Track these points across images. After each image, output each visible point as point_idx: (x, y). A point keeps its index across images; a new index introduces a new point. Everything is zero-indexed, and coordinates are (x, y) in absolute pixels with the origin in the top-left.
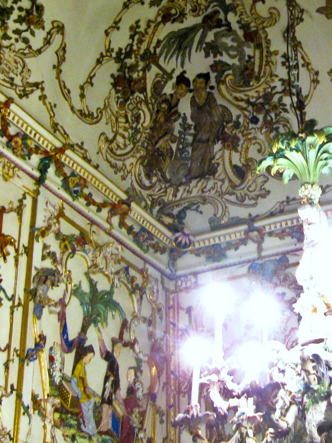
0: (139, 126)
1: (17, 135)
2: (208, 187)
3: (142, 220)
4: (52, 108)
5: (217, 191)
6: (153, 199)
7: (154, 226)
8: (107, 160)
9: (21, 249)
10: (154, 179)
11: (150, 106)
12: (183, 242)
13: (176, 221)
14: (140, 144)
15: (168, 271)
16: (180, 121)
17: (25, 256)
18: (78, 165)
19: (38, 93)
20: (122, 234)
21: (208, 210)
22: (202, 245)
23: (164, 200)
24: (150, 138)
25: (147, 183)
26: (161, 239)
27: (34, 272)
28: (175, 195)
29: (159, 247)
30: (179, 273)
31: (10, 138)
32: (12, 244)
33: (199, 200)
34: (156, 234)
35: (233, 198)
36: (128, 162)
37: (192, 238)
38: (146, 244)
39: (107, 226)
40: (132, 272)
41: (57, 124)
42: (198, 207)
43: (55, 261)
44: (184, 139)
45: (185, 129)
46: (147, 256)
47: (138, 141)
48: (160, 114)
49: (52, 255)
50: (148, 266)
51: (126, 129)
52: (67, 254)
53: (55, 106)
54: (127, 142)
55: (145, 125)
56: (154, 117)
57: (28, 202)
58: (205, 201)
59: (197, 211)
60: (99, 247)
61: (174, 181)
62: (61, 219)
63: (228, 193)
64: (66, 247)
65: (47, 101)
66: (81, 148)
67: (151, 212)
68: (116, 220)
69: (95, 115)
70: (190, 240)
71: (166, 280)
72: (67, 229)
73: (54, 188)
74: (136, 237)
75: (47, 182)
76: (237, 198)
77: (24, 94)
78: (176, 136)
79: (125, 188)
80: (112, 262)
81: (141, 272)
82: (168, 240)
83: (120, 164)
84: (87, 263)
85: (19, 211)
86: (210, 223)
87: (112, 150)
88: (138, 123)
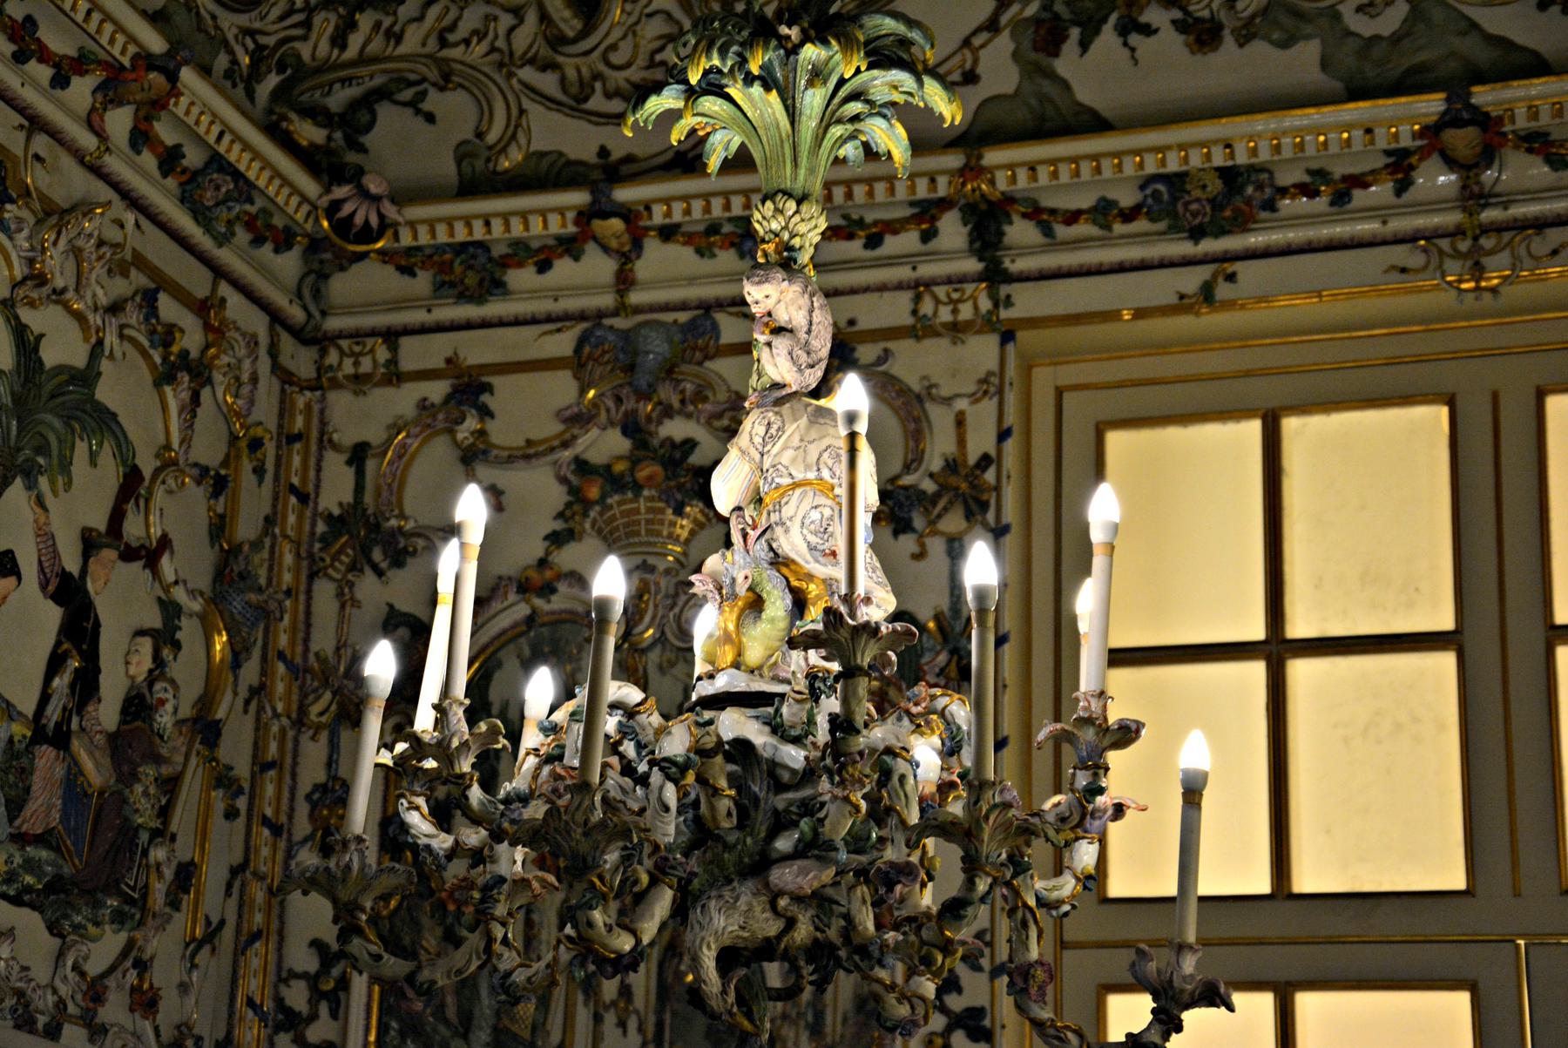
3: (216, 130)
5: (493, 49)
6: (260, 48)
7: (256, 155)
12: (359, 220)
13: (338, 135)
15: (296, 314)
20: (140, 172)
21: (455, 109)
22: (424, 238)
23: (298, 56)
26: (280, 200)
28: (340, 41)
29: (270, 227)
30: (333, 324)
33: (424, 70)
34: (261, 183)
35: (548, 82)
37: (390, 210)
38: (223, 214)
39: (88, 141)
40: (168, 308)
42: (422, 95)
46: (226, 256)
50: (225, 289)
58: (446, 81)
59: (418, 112)
60: (55, 215)
63: (532, 61)
67: (250, 94)
68: (119, 121)
70: (381, 216)
71: (287, 342)
76: (563, 81)
80: (99, 270)
81: (202, 308)
82: (305, 208)
84: (10, 265)
86: (459, 161)
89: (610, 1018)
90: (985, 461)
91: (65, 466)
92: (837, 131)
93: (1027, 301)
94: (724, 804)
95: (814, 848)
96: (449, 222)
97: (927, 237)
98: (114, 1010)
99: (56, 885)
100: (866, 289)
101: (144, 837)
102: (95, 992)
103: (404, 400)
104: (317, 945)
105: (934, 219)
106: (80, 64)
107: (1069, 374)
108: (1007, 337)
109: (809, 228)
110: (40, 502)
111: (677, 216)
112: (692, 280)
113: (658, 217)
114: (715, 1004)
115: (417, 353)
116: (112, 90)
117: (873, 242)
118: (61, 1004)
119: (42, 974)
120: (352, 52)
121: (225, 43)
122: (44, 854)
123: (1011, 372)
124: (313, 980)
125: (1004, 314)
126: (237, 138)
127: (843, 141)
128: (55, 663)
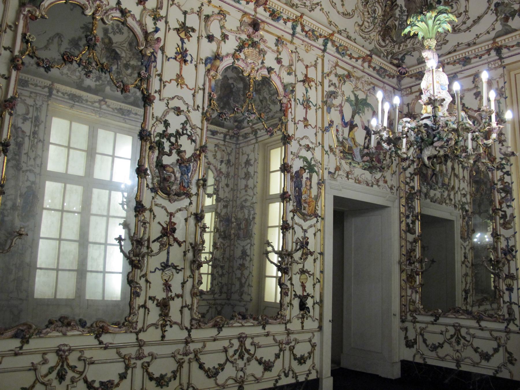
0: (376, 15)
1: (309, 30)
2: (416, 43)
4: (327, 14)
8: (360, 35)
9: (318, 83)
10: (387, 42)
11: (381, 4)
14: (378, 24)
15: (397, 87)
16: (399, 9)
17: (320, 86)
18: (342, 40)
19: (319, 8)
20: (371, 71)
22: (413, 72)
24: (383, 21)
25: (383, 44)
27: (325, 93)
28: (399, 48)
30: (402, 87)
31: (307, 32)
32: (313, 81)
36: (372, 35)
37: (407, 69)
38: (383, 74)
39: (362, 68)
41: (331, 22)
43: (336, 87)
44: (402, 18)
45: (402, 13)
46: (384, 80)
47: (376, 23)
48: (387, 7)
49: (334, 85)
50: (385, 85)
51: (369, 18)
52: (341, 83)
53: (329, 12)
54: (370, 25)
55: (379, 14)
56: (384, 10)
57: (320, 61)
58: (414, 50)
60: (358, 79)
61: (399, 41)
62: (337, 67)
64: (340, 80)
65: (324, 11)
66: (345, 31)
67: (387, 58)
68: (366, 65)
69: (351, 14)
72: (340, 71)
73: (332, 53)
74: (378, 72)
75: (328, 51)
77: (312, 10)
78: (397, 18)
79: (371, 49)
83: (367, 36)
85: (315, 66)
87: (362, 30)
88: (375, 14)
89: (461, 181)
90: (502, 87)
91: (364, 112)
92: (436, 27)
93: (507, 61)
94: (424, 134)
95: (440, 139)
96: (416, 69)
97: (489, 55)
98: (381, 183)
99: (370, 167)
100: (480, 65)
101: (382, 160)
102: (378, 181)
103: (413, 96)
104: (410, 173)
105: (489, 52)
106: (359, 58)
107: (516, 72)
108: (504, 67)
109: (433, 43)
110: (361, 117)
111: (449, 61)
112: (453, 70)
113: (446, 61)
114: (428, 165)
115: (414, 89)
116: (364, 61)
117: (480, 57)
118: (373, 183)
119: (370, 178)
120: (401, 49)
121: (382, 52)
122: (367, 163)
123: (505, 72)
124: (410, 178)
125: (503, 64)
126: (383, 64)
127: (438, 28)
128: (366, 138)
